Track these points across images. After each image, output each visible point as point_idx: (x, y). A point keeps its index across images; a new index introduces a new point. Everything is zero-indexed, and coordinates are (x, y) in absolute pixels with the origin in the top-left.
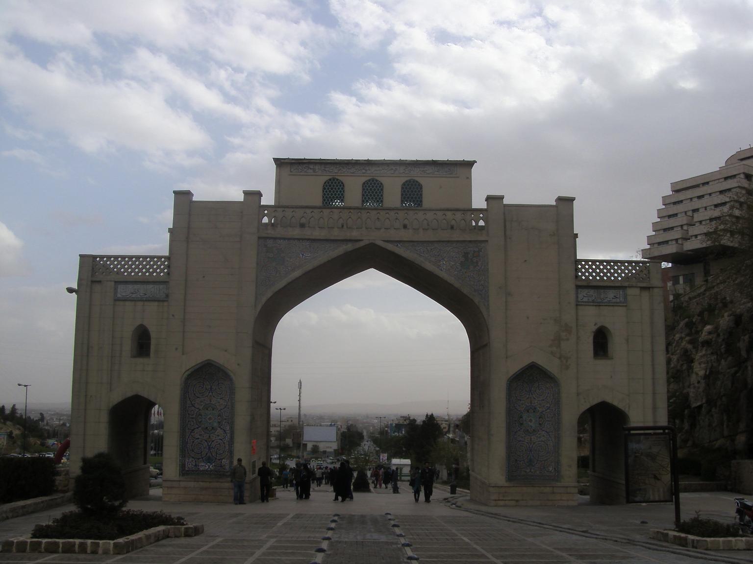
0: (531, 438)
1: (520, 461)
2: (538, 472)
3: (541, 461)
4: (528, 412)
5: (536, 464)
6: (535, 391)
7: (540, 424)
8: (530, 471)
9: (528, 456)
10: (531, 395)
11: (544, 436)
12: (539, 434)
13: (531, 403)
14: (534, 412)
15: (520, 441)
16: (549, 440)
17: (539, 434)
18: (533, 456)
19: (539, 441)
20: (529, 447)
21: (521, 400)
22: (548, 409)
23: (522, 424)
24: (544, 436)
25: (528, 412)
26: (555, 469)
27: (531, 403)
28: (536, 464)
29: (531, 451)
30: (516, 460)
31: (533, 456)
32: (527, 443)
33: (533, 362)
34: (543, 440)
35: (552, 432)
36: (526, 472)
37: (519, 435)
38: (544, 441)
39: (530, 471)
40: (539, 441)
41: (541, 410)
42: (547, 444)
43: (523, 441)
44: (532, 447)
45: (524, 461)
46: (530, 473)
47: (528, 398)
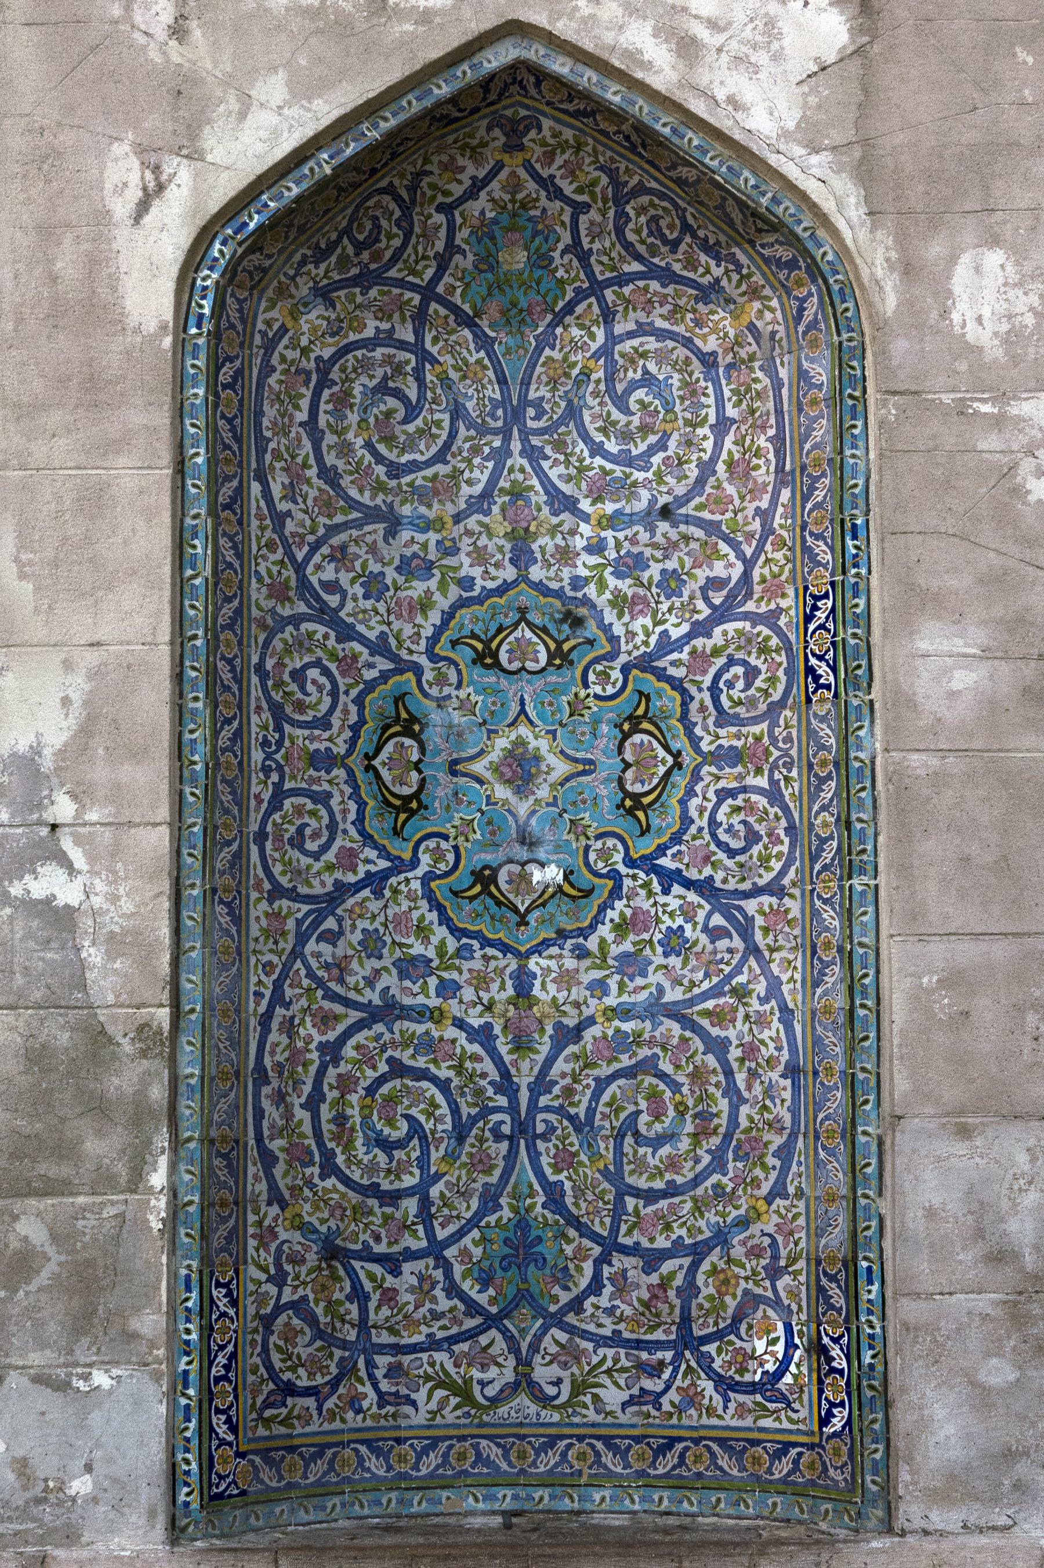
0: (523, 983)
1: (392, 1263)
2: (613, 1396)
3: (652, 1260)
4: (486, 657)
5: (596, 1286)
6: (573, 413)
7: (632, 805)
8: (524, 1382)
9: (490, 1200)
10: (518, 460)
11: (675, 943)
12: (621, 928)
13: (521, 557)
14: (560, 658)
15: (389, 1011)
16: (741, 993)
17: (621, 928)
18: (554, 1197)
19: (624, 1012)
20: (506, 1084)
21: (394, 525)
22: (721, 614)
23: (409, 806)
24: (675, 943)
25: (486, 657)
26: (819, 1350)
27: (521, 557)
28: (596, 1286)
29: (523, 1128)
30: (333, 1252)
31: (554, 1197)
32: (484, 1035)
33: (514, 29)
34: (673, 995)
35: (775, 889)
36: (463, 1391)
37: (372, 945)
38: (674, 1012)
39: (524, 1382)
40: (624, 1012)
41: (638, 632)
42: (719, 1047)
43: (422, 1014)
44: (541, 1084)
45: (435, 1250)
46: (525, 1404)
47: (482, 502)
